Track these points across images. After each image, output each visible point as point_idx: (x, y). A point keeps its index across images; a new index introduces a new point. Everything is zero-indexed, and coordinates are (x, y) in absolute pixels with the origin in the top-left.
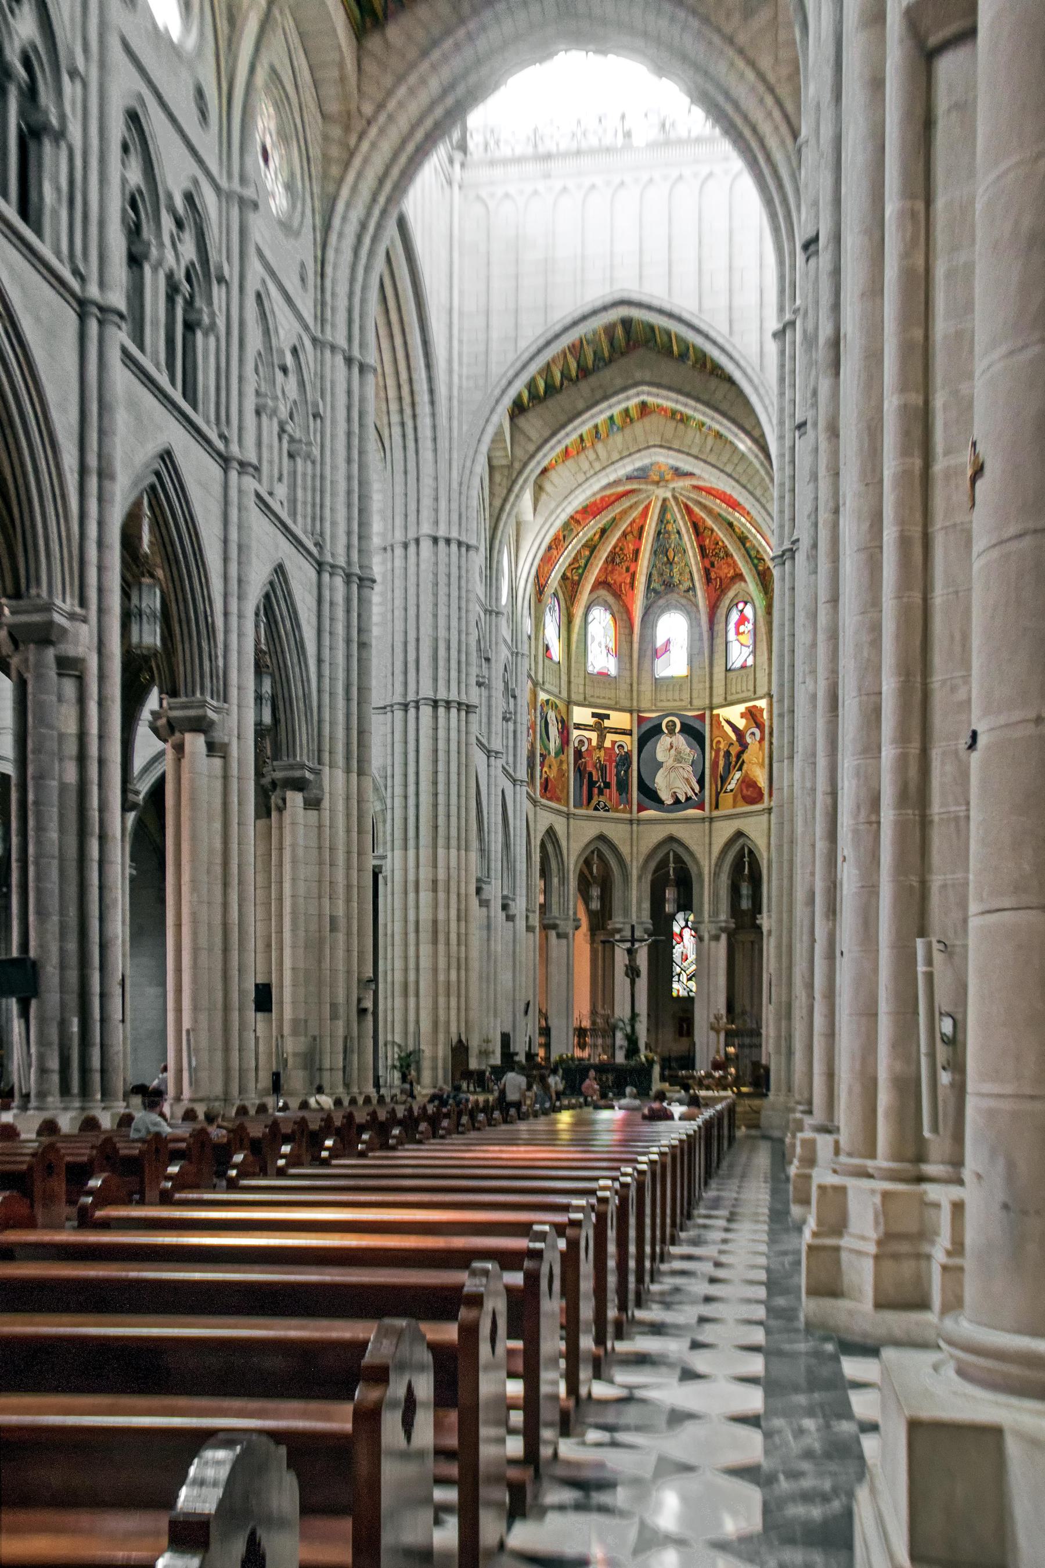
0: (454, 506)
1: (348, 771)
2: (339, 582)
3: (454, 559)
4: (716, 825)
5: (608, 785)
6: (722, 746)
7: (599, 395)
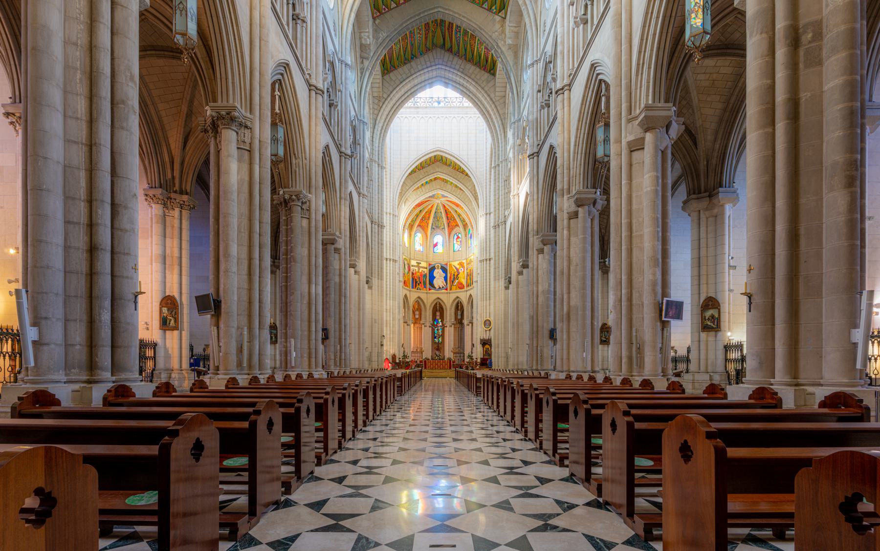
0: (392, 204)
1: (378, 279)
2: (376, 226)
3: (392, 219)
4: (451, 295)
5: (420, 283)
6: (453, 273)
7: (426, 174)
